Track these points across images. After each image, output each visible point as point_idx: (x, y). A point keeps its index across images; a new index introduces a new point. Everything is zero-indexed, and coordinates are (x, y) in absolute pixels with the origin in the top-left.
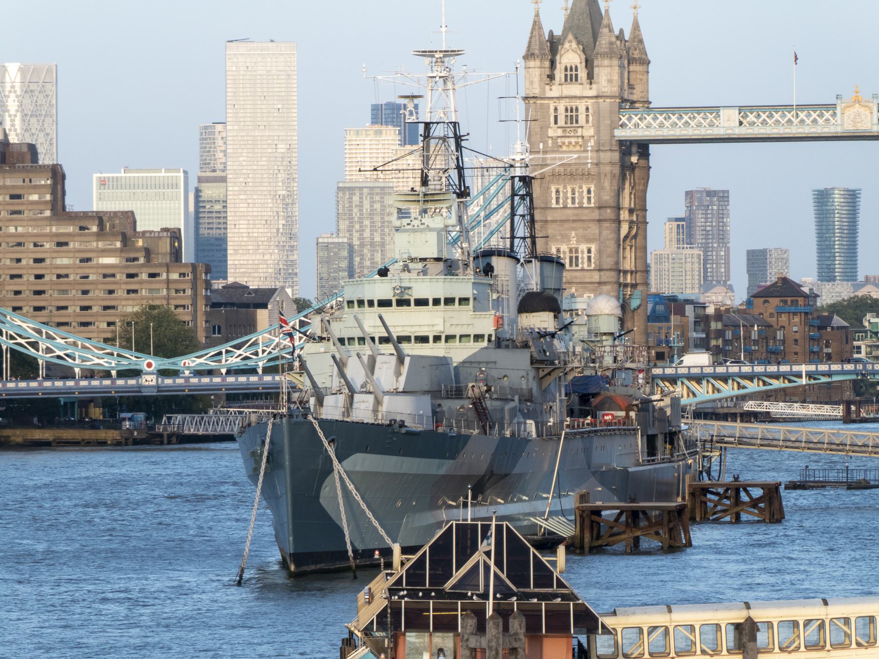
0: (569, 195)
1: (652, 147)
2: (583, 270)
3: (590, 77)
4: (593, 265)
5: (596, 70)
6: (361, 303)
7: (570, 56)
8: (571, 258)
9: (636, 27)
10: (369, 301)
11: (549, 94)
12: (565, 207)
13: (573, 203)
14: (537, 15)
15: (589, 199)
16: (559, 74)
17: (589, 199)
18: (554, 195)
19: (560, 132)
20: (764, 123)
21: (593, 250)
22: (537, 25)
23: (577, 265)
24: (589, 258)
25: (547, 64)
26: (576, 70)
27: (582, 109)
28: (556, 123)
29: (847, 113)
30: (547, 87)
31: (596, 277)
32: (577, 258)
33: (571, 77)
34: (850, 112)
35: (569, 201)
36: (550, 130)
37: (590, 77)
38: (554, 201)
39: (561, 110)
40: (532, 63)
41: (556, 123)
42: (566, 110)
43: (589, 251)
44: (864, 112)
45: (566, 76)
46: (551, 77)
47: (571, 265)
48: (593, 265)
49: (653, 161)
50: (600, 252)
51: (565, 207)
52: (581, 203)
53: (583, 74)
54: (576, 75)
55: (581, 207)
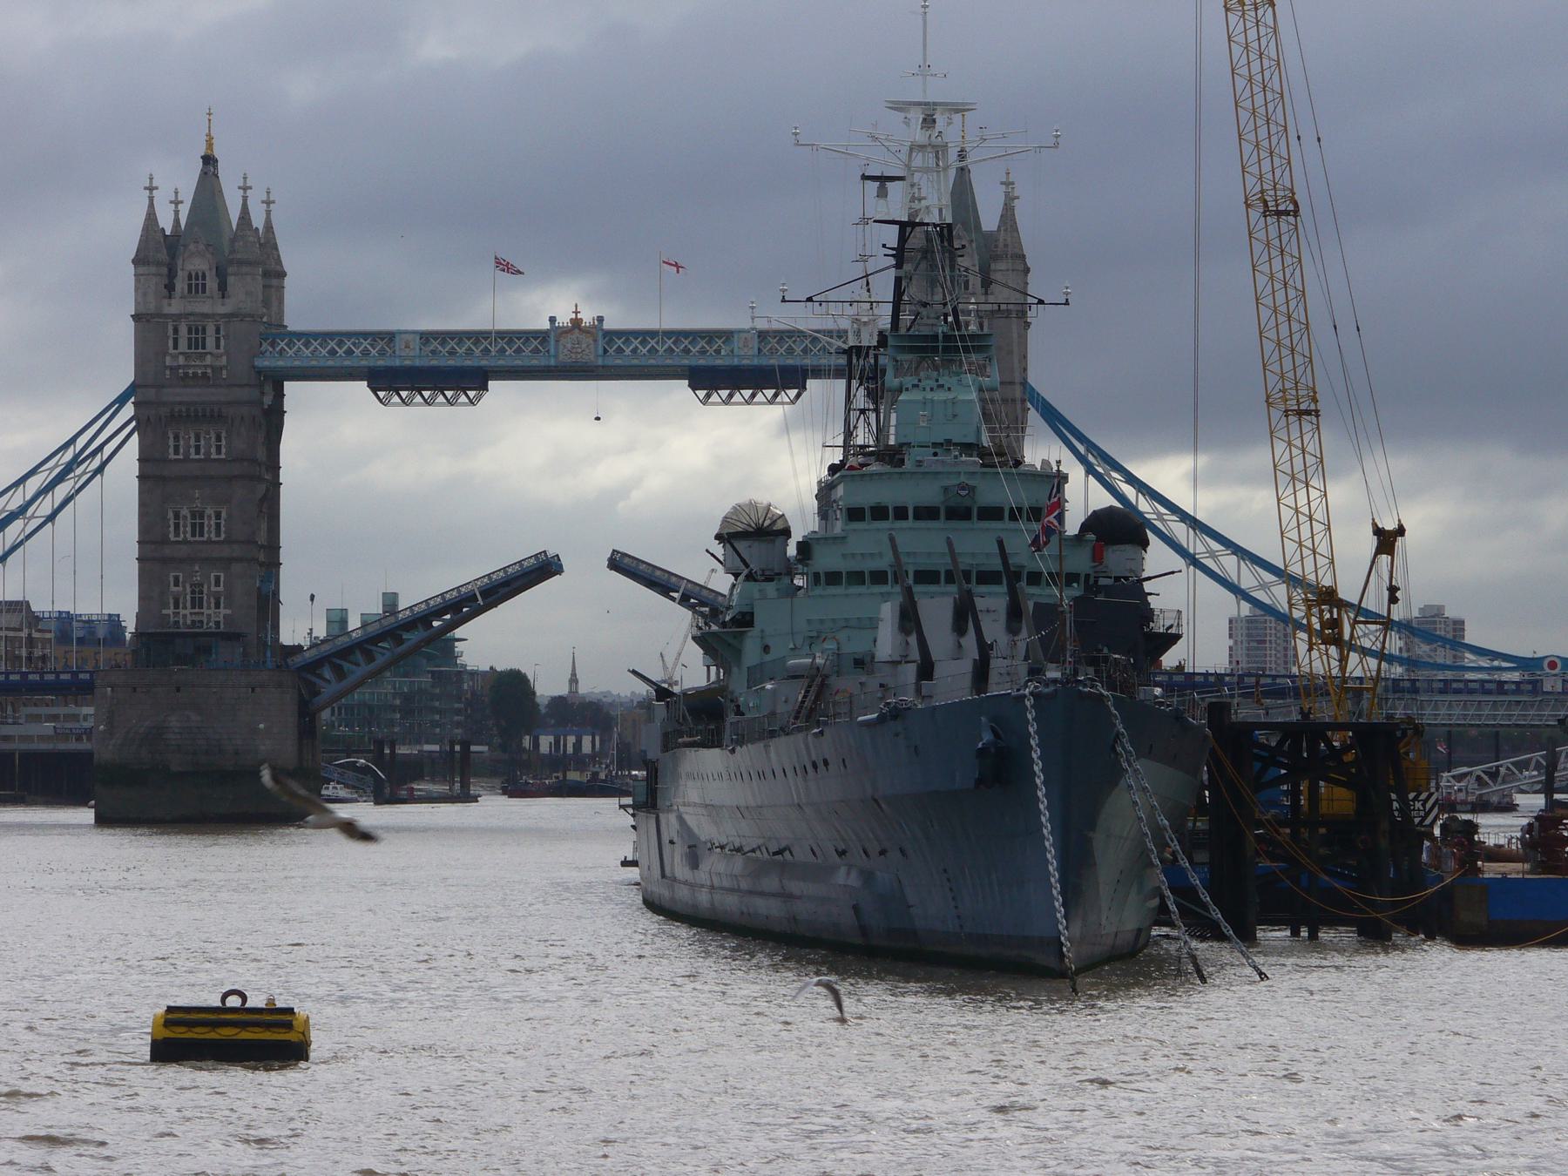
0: (192, 442)
1: (288, 386)
2: (210, 542)
3: (223, 288)
4: (223, 536)
5: (231, 280)
6: (879, 513)
7: (196, 263)
8: (193, 526)
9: (269, 227)
10: (896, 509)
11: (167, 310)
12: (187, 459)
13: (198, 452)
14: (151, 205)
15: (219, 449)
16: (181, 285)
17: (219, 449)
18: (171, 442)
19: (181, 360)
20: (452, 353)
21: (224, 515)
22: (151, 217)
23: (202, 535)
24: (218, 526)
25: (165, 270)
26: (204, 277)
27: (211, 329)
28: (176, 347)
29: (563, 341)
30: (166, 301)
31: (226, 551)
32: (202, 525)
33: (196, 286)
34: (567, 342)
35: (192, 450)
36: (168, 359)
37: (223, 288)
38: (171, 450)
39: (183, 330)
40: (142, 270)
41: (176, 347)
42: (190, 332)
43: (218, 516)
44: (586, 341)
45: (190, 286)
46: (170, 288)
47: (193, 535)
48: (223, 536)
49: (288, 404)
50: (229, 516)
51: (187, 459)
52: (208, 453)
53: (212, 284)
54: (204, 285)
55: (208, 459)
